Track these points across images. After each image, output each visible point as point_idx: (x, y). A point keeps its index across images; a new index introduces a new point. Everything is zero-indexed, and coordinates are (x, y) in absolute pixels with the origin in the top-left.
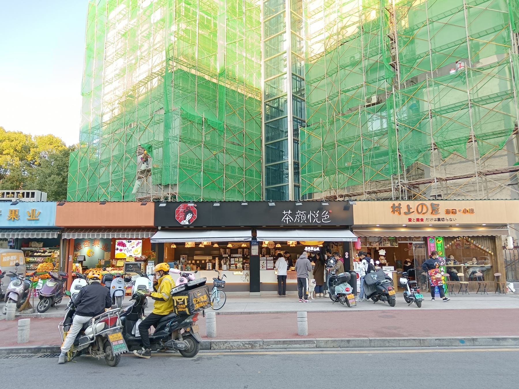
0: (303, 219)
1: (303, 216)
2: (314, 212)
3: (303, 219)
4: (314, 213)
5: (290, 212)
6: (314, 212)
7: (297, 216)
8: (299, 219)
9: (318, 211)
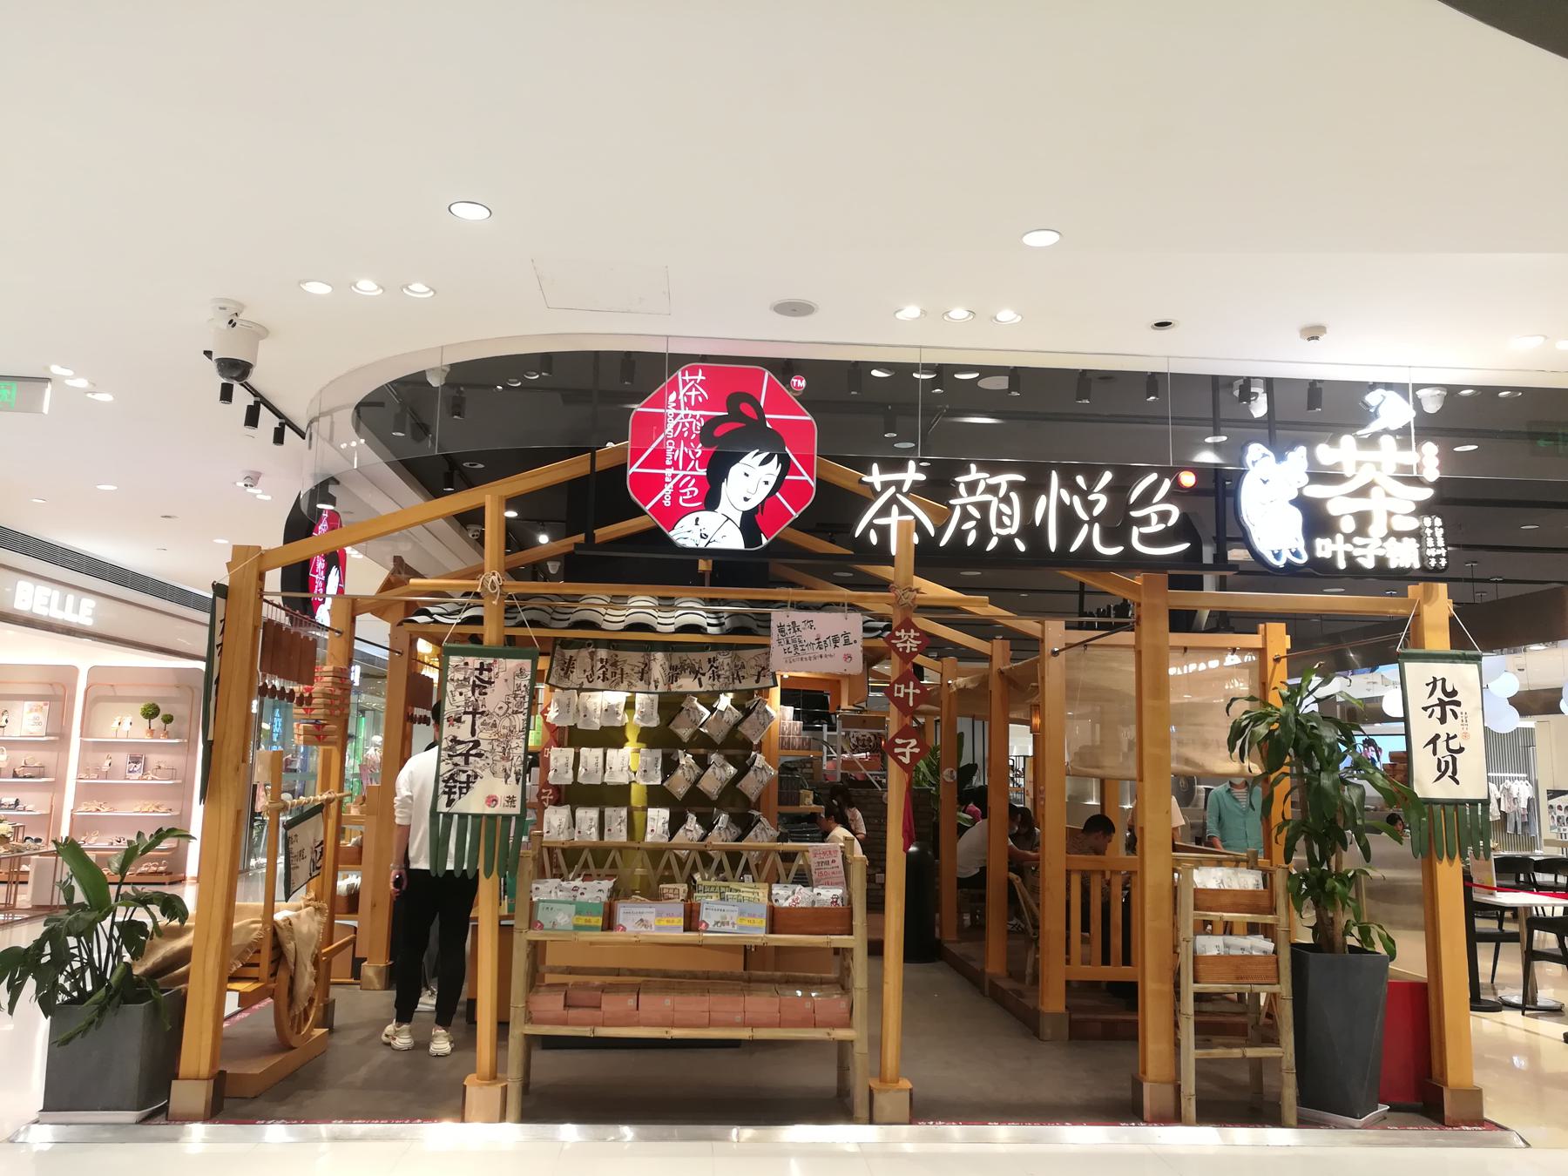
0: (1001, 524)
1: (1005, 508)
2: (1080, 480)
3: (1001, 524)
4: (1074, 489)
5: (912, 475)
6: (1080, 480)
7: (963, 507)
8: (972, 524)
9: (1107, 477)
